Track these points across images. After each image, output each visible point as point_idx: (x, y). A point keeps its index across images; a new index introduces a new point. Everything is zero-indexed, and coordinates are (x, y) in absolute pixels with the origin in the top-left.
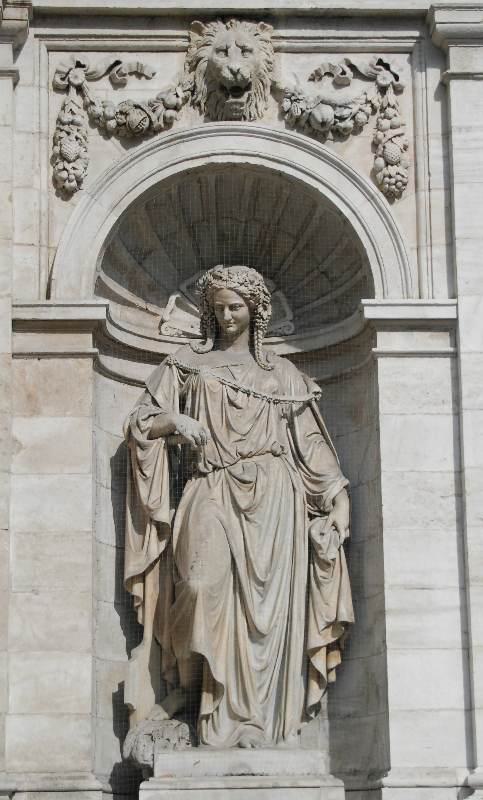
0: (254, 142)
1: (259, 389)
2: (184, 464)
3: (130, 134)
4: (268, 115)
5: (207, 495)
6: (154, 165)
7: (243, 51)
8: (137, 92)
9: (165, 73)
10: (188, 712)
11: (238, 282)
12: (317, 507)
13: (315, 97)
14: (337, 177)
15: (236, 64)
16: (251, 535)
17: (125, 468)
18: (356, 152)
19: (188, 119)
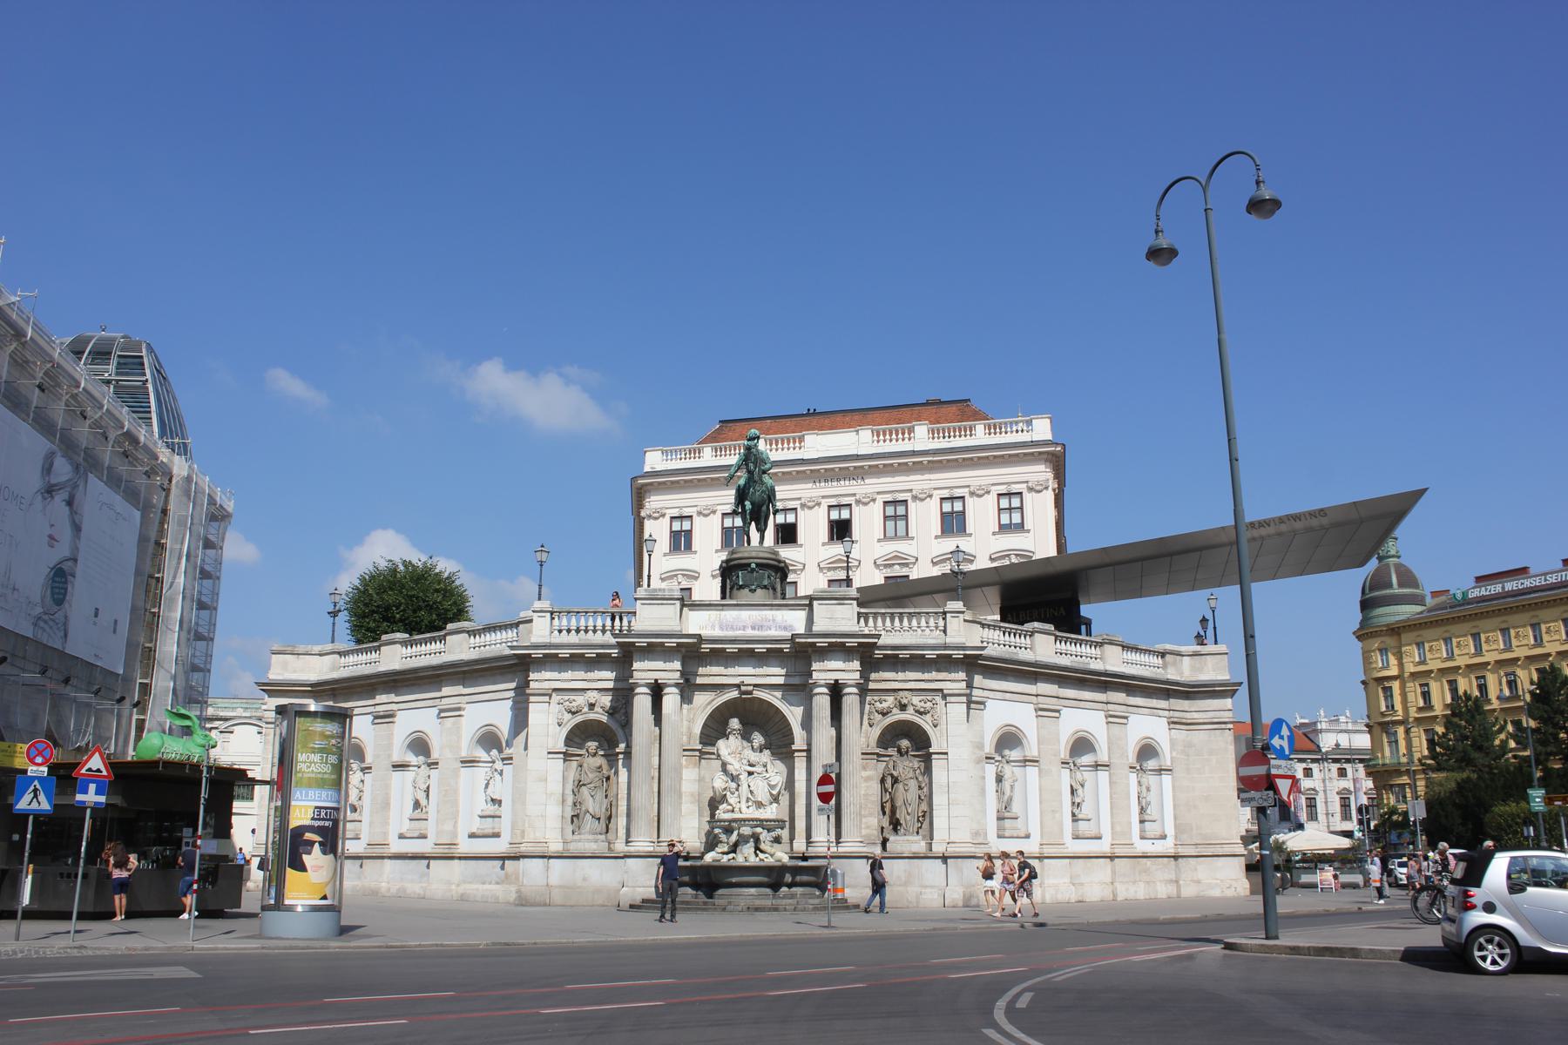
0: (909, 716)
1: (907, 767)
2: (895, 781)
3: (884, 714)
4: (910, 710)
5: (900, 786)
6: (889, 720)
7: (905, 697)
8: (885, 705)
9: (890, 701)
10: (895, 830)
11: (905, 743)
12: (920, 788)
13: (920, 705)
14: (925, 723)
15: (904, 701)
16: (908, 794)
17: (883, 781)
18: (928, 717)
19: (895, 711)
